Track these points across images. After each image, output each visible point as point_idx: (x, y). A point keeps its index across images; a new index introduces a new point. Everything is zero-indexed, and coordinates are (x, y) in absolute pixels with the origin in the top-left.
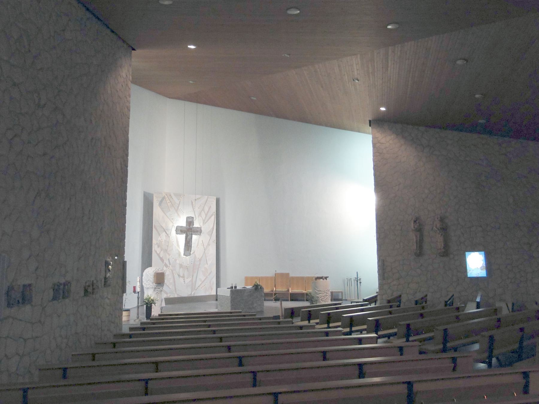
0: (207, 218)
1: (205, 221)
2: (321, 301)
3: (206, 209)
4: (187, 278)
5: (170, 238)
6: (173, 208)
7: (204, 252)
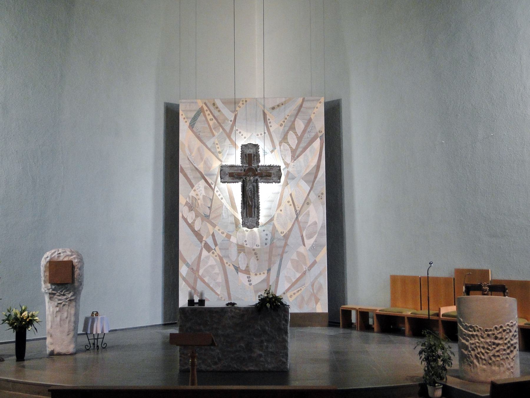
0: (303, 145)
1: (298, 152)
2: (475, 361)
3: (300, 125)
4: (256, 275)
5: (215, 192)
6: (221, 130)
7: (297, 218)
